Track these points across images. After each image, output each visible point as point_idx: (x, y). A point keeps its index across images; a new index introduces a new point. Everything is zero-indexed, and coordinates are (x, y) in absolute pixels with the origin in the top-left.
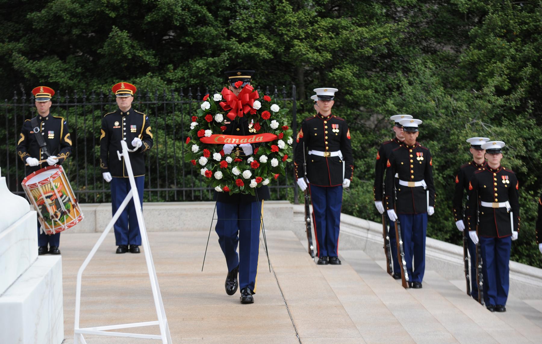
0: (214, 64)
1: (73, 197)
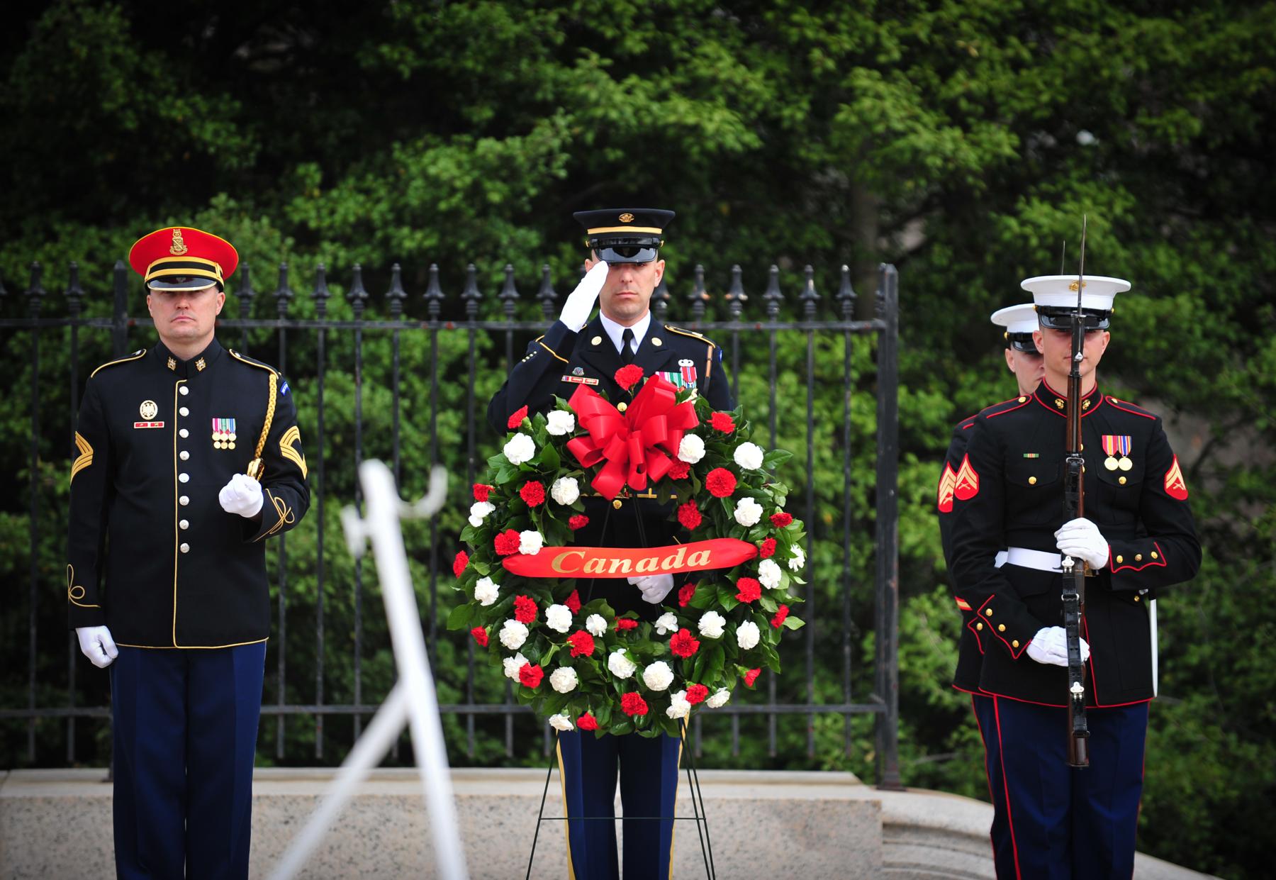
0: (506, 169)
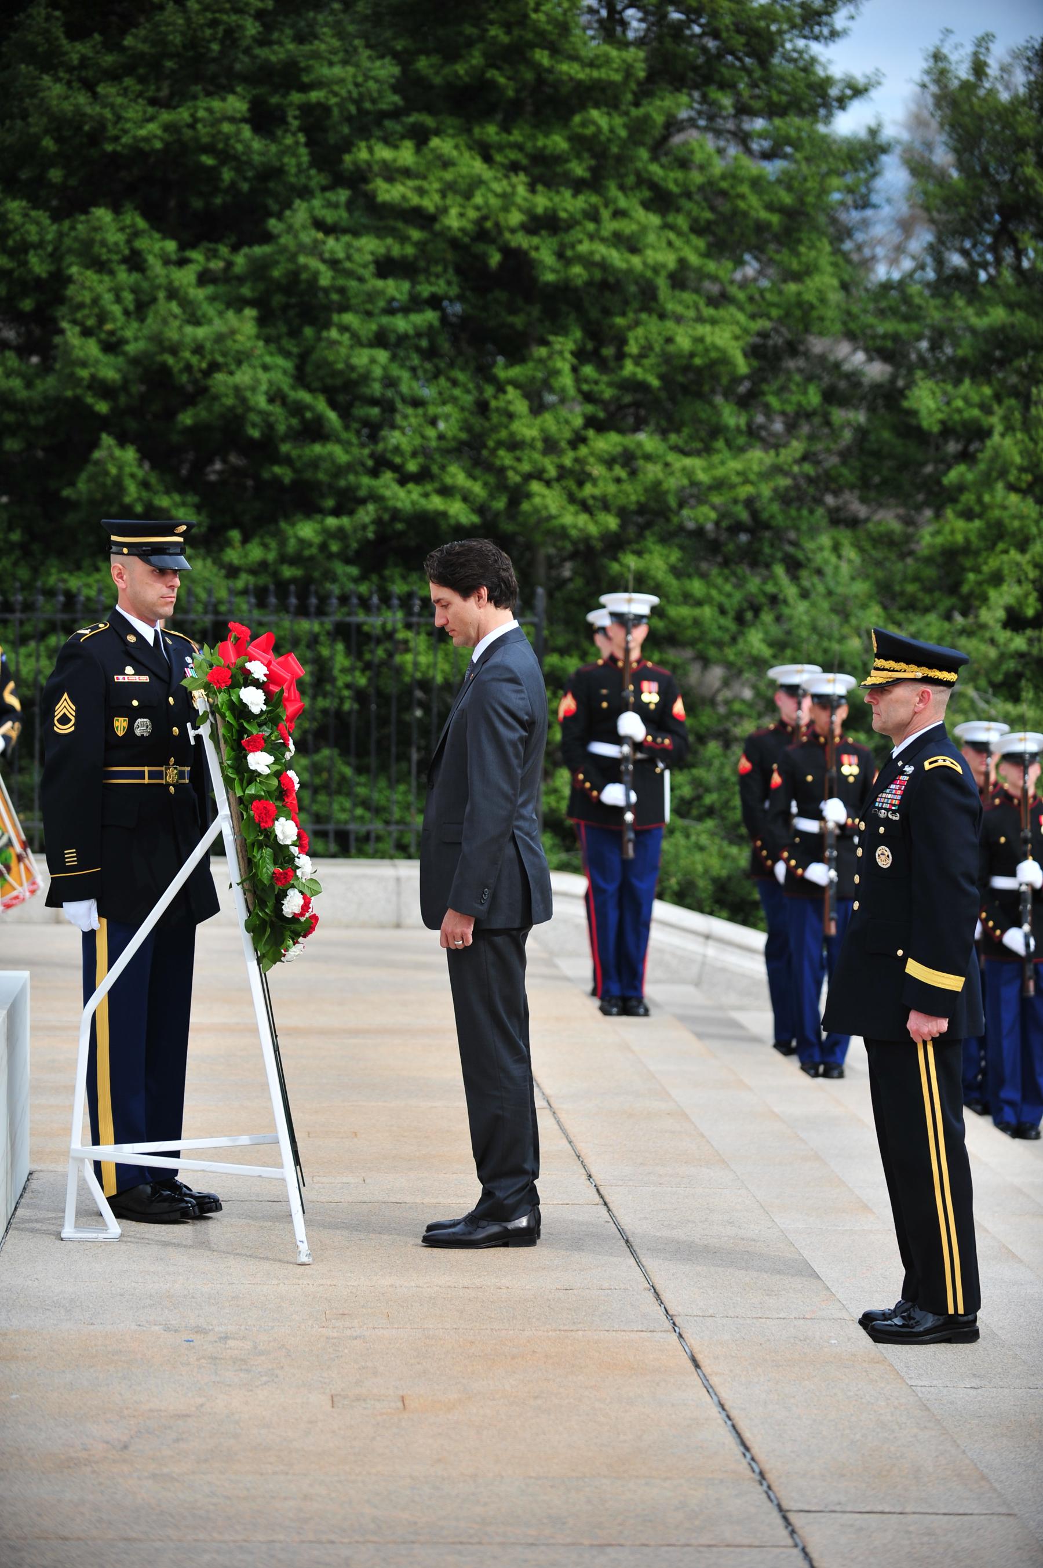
0: (340, 534)
1: (18, 835)
